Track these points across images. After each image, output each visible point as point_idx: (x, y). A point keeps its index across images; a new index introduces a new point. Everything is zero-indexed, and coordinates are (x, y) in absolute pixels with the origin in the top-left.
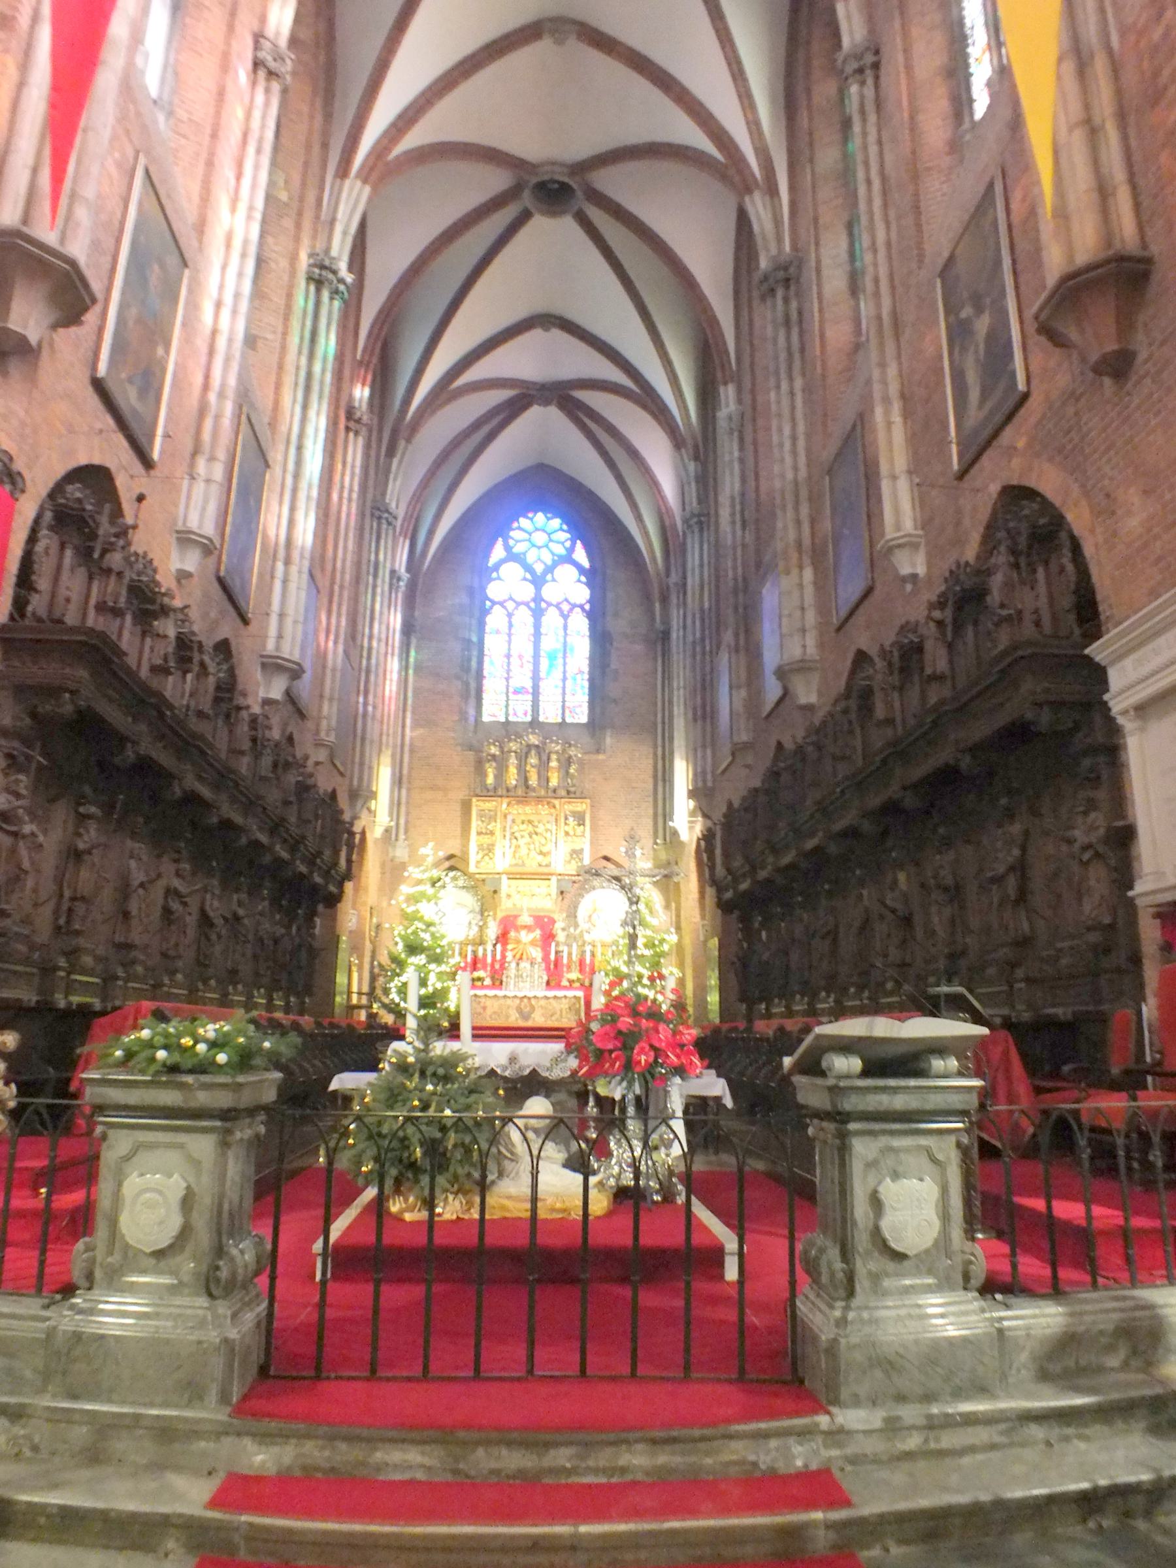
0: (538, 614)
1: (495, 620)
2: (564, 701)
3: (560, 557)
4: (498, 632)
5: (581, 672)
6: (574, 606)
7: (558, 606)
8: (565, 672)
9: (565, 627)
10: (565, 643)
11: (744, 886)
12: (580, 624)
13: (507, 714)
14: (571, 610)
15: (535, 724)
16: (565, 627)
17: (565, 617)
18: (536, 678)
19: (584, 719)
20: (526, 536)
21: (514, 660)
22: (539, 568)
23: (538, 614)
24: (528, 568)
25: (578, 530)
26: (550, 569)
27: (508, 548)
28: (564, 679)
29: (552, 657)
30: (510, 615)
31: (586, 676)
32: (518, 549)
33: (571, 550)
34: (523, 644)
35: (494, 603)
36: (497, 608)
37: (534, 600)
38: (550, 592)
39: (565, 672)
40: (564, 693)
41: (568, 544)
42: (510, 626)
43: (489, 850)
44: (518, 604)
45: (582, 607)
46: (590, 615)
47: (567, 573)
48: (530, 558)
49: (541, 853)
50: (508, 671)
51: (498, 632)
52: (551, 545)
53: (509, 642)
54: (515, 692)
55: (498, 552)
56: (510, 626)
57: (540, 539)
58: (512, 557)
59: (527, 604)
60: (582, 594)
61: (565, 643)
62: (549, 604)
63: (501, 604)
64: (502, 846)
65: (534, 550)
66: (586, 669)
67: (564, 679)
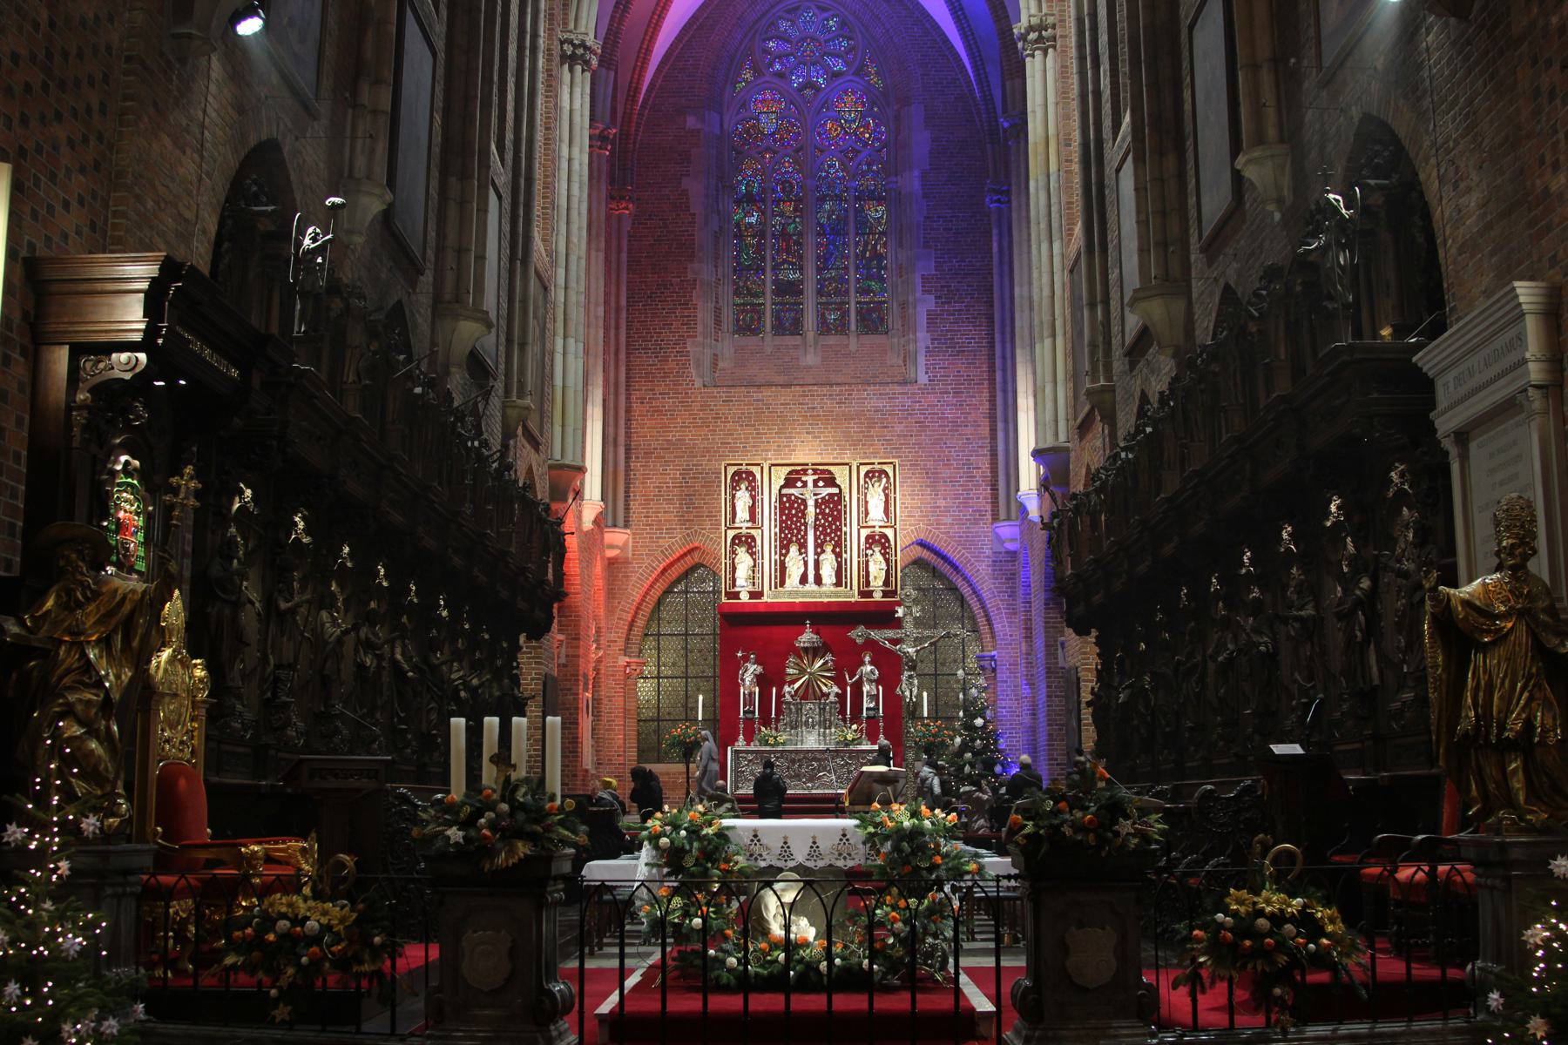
11: (1097, 599)
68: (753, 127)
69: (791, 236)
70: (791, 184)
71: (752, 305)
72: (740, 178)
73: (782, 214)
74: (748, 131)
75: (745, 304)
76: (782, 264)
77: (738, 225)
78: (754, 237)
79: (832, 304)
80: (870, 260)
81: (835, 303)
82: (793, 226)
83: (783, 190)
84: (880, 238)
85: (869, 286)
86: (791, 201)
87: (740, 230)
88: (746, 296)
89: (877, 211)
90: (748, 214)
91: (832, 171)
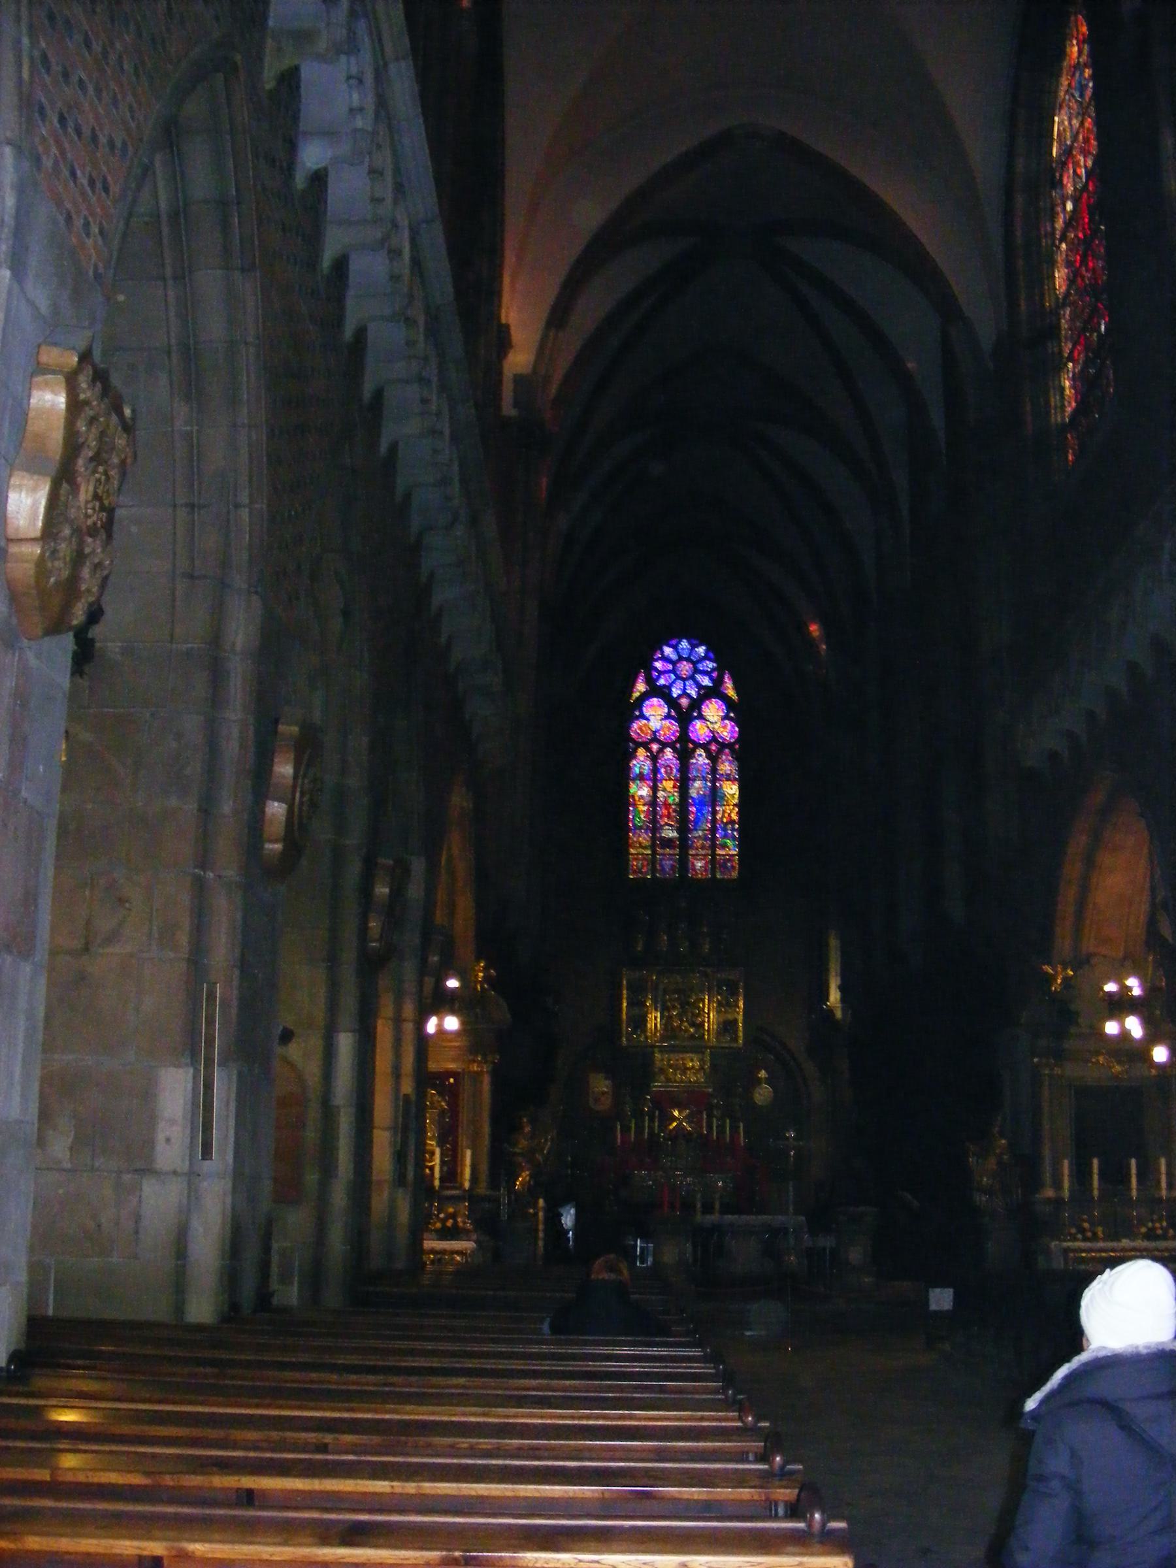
0: (685, 753)
1: (640, 763)
2: (714, 855)
3: (706, 687)
4: (641, 777)
5: (732, 822)
6: (723, 745)
7: (705, 747)
8: (714, 821)
9: (714, 771)
10: (714, 788)
12: (726, 766)
13: (654, 871)
14: (720, 752)
15: (684, 882)
16: (714, 771)
17: (714, 759)
18: (684, 827)
19: (735, 874)
20: (670, 667)
21: (661, 811)
22: (684, 702)
23: (685, 753)
24: (672, 703)
25: (725, 660)
26: (696, 705)
27: (650, 681)
28: (713, 830)
29: (701, 803)
30: (654, 758)
31: (737, 826)
32: (662, 682)
33: (718, 682)
34: (668, 790)
35: (639, 745)
36: (641, 752)
37: (679, 740)
38: (700, 730)
39: (714, 821)
40: (713, 847)
41: (715, 675)
42: (655, 770)
43: (640, 1022)
44: (664, 745)
45: (730, 746)
46: (740, 758)
47: (713, 711)
48: (676, 692)
49: (693, 1025)
50: (654, 821)
51: (641, 777)
52: (698, 677)
53: (655, 789)
54: (663, 846)
55: (641, 687)
56: (655, 770)
57: (685, 668)
58: (655, 691)
59: (672, 745)
60: (727, 731)
61: (714, 788)
62: (697, 745)
63: (646, 745)
64: (654, 1019)
65: (680, 684)
66: (735, 817)
67: (713, 830)
68: (645, 725)
69: (670, 805)
70: (670, 767)
71: (643, 854)
72: (634, 762)
73: (664, 790)
74: (640, 729)
75: (637, 854)
76: (664, 825)
77: (633, 797)
78: (644, 805)
79: (697, 855)
80: (727, 824)
81: (702, 855)
82: (672, 798)
83: (666, 772)
84: (733, 809)
85: (726, 843)
86: (670, 779)
87: (634, 800)
88: (638, 848)
89: (731, 789)
90: (640, 788)
91: (700, 759)
